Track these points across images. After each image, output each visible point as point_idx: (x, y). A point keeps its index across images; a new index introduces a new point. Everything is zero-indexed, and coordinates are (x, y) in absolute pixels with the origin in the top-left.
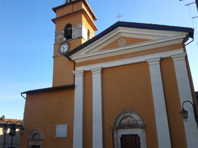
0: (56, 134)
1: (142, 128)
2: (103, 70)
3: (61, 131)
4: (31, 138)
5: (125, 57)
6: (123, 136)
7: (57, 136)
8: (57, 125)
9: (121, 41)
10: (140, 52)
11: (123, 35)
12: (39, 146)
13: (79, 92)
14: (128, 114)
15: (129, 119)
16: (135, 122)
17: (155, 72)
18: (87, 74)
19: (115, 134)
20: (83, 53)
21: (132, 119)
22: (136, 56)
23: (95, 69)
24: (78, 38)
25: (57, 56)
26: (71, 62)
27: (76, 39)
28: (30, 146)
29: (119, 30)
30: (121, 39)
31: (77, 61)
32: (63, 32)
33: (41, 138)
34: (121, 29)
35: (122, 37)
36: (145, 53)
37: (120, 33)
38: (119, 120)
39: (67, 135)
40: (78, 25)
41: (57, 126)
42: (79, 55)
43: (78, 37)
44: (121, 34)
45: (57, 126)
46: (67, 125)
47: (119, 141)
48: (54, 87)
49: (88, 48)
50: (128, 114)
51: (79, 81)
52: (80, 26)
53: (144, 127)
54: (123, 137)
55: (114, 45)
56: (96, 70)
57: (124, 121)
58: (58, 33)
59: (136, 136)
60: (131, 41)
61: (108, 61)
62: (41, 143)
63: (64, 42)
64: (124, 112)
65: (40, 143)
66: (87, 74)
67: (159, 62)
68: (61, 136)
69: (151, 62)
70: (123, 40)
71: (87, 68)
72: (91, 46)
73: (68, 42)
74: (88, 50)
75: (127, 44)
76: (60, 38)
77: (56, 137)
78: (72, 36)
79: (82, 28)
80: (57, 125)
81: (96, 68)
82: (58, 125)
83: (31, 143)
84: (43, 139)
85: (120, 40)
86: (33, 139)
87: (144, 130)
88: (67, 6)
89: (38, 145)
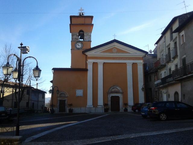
1: (122, 93)
3: (79, 93)
4: (59, 95)
11: (115, 47)
12: (65, 100)
13: (90, 74)
14: (115, 87)
15: (115, 89)
18: (95, 65)
19: (109, 96)
20: (93, 52)
24: (89, 41)
31: (88, 56)
33: (66, 96)
34: (115, 44)
35: (115, 47)
38: (111, 89)
47: (110, 99)
50: (115, 87)
51: (90, 67)
52: (89, 34)
53: (122, 93)
54: (112, 97)
55: (110, 51)
57: (113, 90)
59: (118, 96)
66: (95, 65)
68: (79, 95)
75: (116, 53)
76: (76, 38)
79: (91, 35)
81: (100, 62)
83: (59, 99)
86: (60, 97)
88: (81, 18)
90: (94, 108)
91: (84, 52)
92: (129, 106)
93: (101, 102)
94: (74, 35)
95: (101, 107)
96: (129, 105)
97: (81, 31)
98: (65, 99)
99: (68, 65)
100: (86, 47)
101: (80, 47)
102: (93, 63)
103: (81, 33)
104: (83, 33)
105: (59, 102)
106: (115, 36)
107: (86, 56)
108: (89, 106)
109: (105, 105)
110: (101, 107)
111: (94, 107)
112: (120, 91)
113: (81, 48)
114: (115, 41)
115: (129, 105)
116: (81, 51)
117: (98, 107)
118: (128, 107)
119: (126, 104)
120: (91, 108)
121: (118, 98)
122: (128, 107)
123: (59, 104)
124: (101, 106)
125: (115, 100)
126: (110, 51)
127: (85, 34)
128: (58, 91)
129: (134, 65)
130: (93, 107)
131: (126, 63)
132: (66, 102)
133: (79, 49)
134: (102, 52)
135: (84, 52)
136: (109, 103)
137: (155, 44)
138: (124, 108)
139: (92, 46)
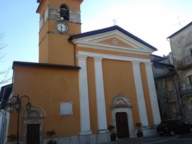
0: (60, 112)
1: (130, 108)
2: (104, 60)
3: (66, 108)
5: (119, 54)
6: (117, 113)
7: (61, 114)
8: (60, 103)
9: (116, 40)
10: (139, 55)
12: (39, 125)
13: (83, 75)
14: (120, 97)
16: (125, 103)
17: (136, 69)
20: (87, 40)
21: (123, 101)
22: (125, 56)
23: (84, 55)
24: (78, 23)
25: (53, 32)
26: (70, 43)
27: (75, 23)
28: (26, 125)
29: (116, 32)
30: (115, 39)
31: (78, 46)
32: (59, 10)
33: (42, 116)
34: (117, 32)
35: (115, 38)
36: (130, 56)
37: (115, 34)
39: (72, 113)
40: (76, 11)
41: (61, 104)
42: (84, 40)
43: (78, 22)
44: (116, 35)
45: (61, 104)
46: (72, 103)
47: (115, 117)
48: (40, 63)
49: (93, 37)
50: (120, 97)
51: (82, 63)
52: (78, 13)
53: (131, 107)
54: (118, 114)
56: (99, 58)
57: (118, 103)
58: (52, 8)
59: (125, 113)
60: (121, 43)
61: (108, 54)
62: (42, 121)
63: (62, 21)
64: (119, 96)
65: (40, 121)
67: (101, 61)
68: (66, 113)
69: (147, 64)
70: (116, 40)
71: (91, 55)
72: (95, 37)
73: (66, 22)
74: (92, 39)
75: (117, 45)
76: (56, 15)
77: (61, 115)
78: (70, 19)
79: (80, 15)
80: (60, 103)
81: (98, 57)
82: (62, 103)
83: (26, 122)
84: (45, 117)
85: (114, 40)
86: (29, 118)
87: (131, 109)
89: (37, 123)
90: (94, 136)
91: (70, 39)
92: (144, 127)
93: (103, 124)
94: (52, 10)
95: (104, 132)
96: (143, 125)
97: (63, 6)
98: (40, 121)
99: (35, 59)
100: (73, 32)
101: (64, 30)
102: (87, 57)
103: (64, 9)
104: (66, 10)
105: (26, 128)
106: (114, 20)
107: (75, 45)
108: (85, 132)
109: (110, 128)
110: (104, 132)
111: (93, 133)
112: (128, 104)
113: (66, 33)
114: (116, 28)
115: (143, 125)
116: (69, 37)
117: (100, 132)
118: (143, 128)
119: (138, 125)
120: (89, 135)
121: (125, 114)
122: (143, 128)
123: (26, 132)
124: (105, 130)
125: (122, 118)
126: (109, 41)
127: (70, 11)
128: (29, 104)
129: (142, 64)
130: (91, 133)
131: (130, 62)
132: (41, 129)
133: (61, 33)
134: (99, 42)
135: (70, 39)
136: (114, 124)
137: (167, 39)
138: (136, 132)
139: (84, 29)
